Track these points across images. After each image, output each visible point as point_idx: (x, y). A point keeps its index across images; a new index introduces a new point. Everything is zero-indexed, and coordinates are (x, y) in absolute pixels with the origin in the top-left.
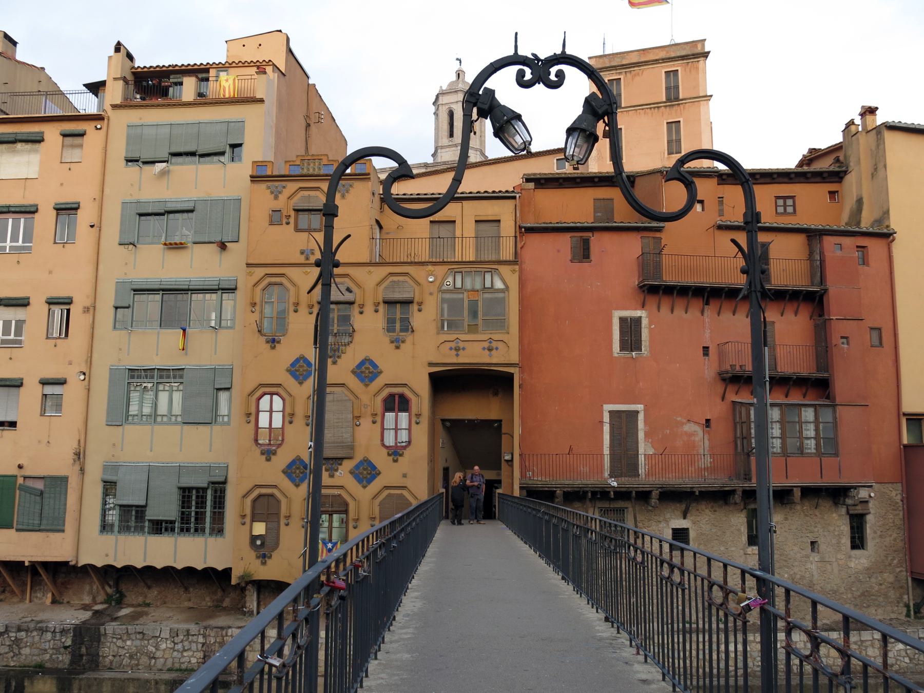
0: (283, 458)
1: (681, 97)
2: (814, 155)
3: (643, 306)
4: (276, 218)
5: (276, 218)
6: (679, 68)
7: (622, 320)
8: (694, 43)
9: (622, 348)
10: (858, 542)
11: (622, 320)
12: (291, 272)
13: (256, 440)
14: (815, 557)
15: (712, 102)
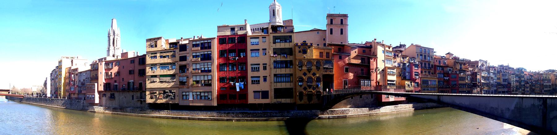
0: (303, 87)
1: (343, 24)
2: (367, 43)
3: (348, 66)
4: (300, 52)
5: (300, 52)
6: (343, 19)
7: (346, 68)
8: (345, 15)
9: (346, 72)
10: (372, 97)
11: (346, 68)
12: (302, 60)
13: (299, 84)
14: (367, 99)
15: (348, 26)
